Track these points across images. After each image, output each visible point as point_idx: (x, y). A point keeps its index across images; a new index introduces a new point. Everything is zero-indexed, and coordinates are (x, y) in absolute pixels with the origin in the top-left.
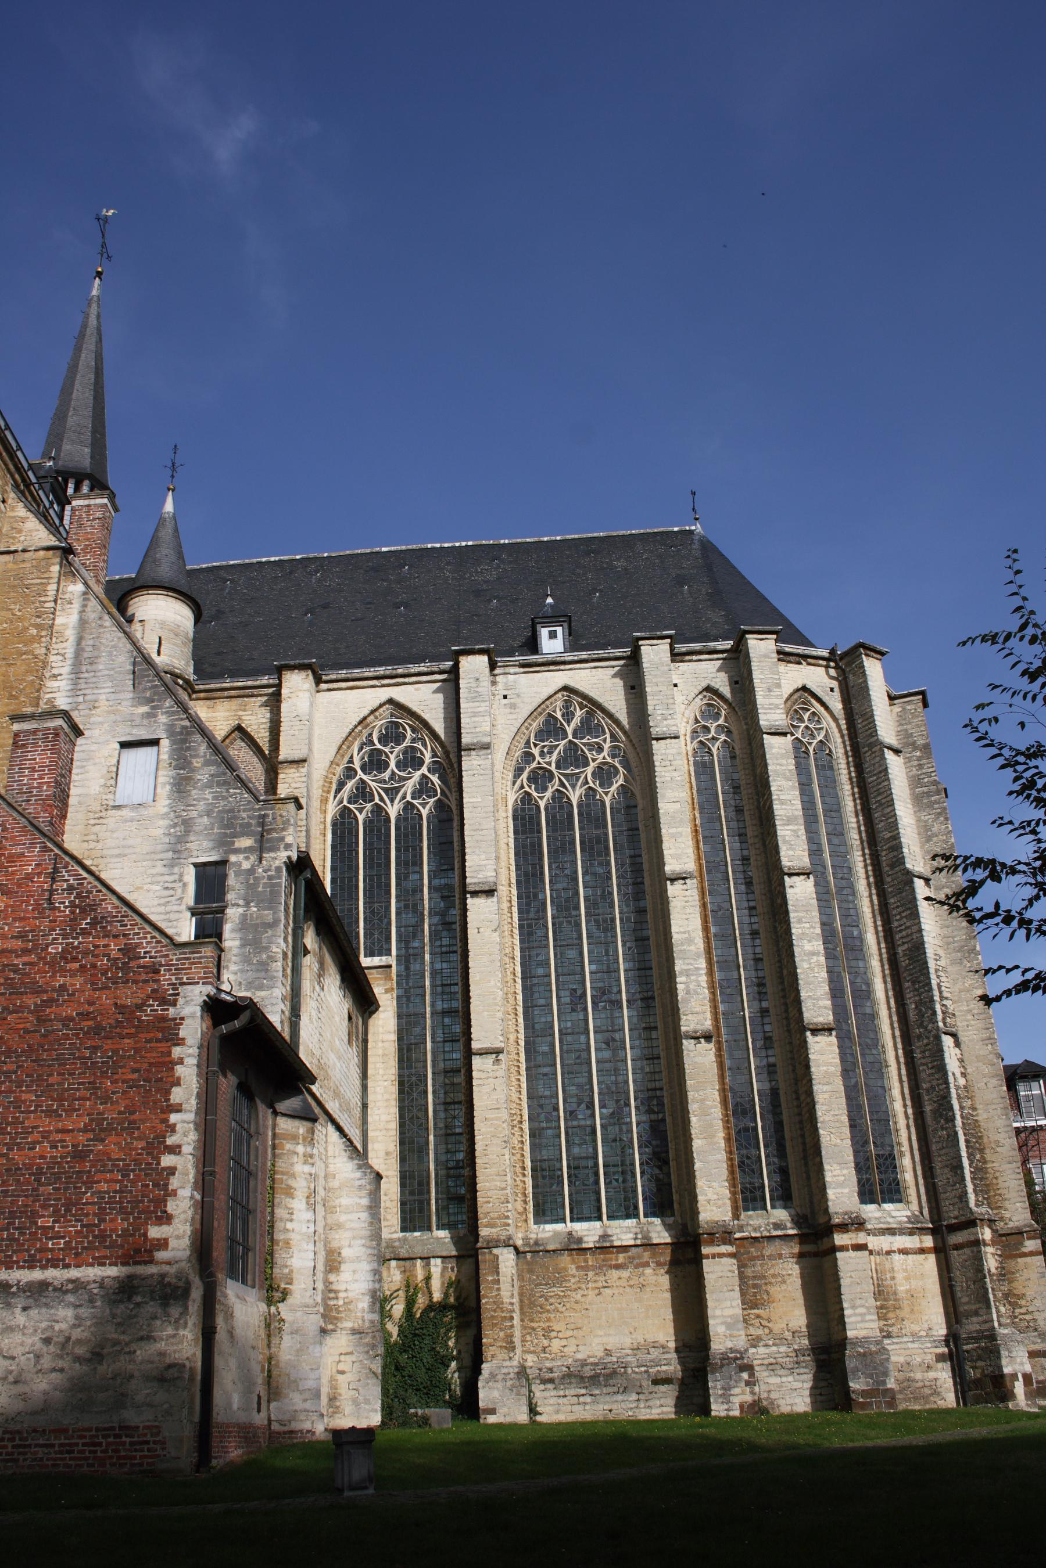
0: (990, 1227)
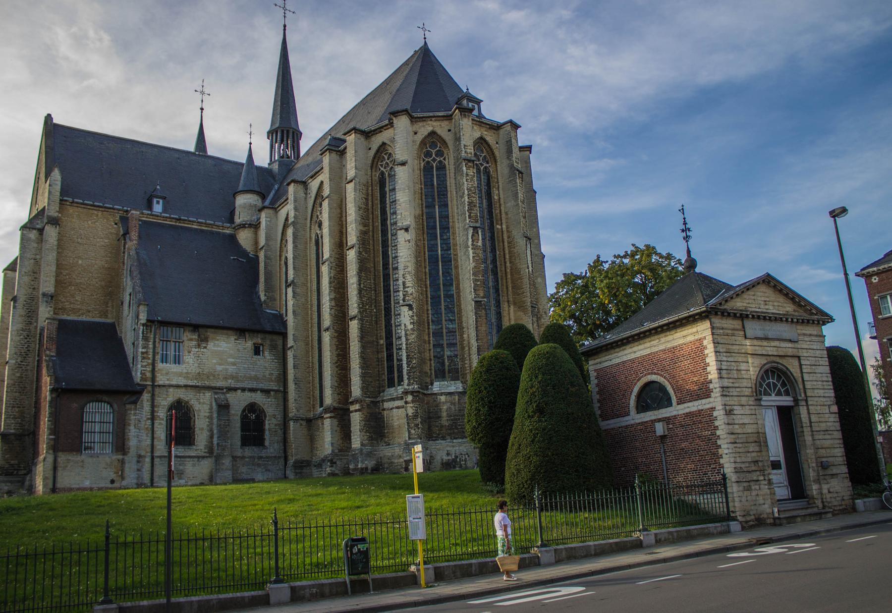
0: (411, 395)
